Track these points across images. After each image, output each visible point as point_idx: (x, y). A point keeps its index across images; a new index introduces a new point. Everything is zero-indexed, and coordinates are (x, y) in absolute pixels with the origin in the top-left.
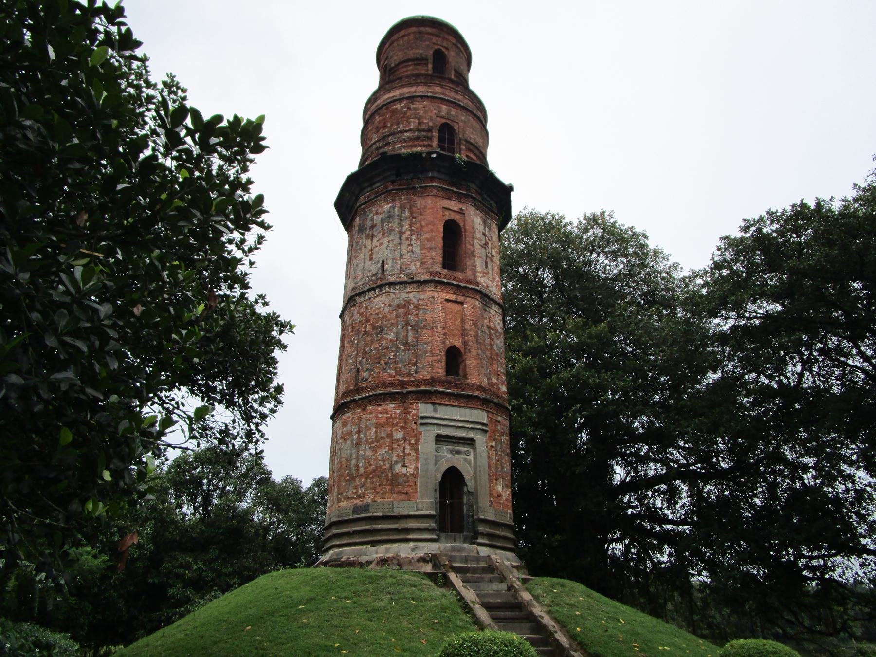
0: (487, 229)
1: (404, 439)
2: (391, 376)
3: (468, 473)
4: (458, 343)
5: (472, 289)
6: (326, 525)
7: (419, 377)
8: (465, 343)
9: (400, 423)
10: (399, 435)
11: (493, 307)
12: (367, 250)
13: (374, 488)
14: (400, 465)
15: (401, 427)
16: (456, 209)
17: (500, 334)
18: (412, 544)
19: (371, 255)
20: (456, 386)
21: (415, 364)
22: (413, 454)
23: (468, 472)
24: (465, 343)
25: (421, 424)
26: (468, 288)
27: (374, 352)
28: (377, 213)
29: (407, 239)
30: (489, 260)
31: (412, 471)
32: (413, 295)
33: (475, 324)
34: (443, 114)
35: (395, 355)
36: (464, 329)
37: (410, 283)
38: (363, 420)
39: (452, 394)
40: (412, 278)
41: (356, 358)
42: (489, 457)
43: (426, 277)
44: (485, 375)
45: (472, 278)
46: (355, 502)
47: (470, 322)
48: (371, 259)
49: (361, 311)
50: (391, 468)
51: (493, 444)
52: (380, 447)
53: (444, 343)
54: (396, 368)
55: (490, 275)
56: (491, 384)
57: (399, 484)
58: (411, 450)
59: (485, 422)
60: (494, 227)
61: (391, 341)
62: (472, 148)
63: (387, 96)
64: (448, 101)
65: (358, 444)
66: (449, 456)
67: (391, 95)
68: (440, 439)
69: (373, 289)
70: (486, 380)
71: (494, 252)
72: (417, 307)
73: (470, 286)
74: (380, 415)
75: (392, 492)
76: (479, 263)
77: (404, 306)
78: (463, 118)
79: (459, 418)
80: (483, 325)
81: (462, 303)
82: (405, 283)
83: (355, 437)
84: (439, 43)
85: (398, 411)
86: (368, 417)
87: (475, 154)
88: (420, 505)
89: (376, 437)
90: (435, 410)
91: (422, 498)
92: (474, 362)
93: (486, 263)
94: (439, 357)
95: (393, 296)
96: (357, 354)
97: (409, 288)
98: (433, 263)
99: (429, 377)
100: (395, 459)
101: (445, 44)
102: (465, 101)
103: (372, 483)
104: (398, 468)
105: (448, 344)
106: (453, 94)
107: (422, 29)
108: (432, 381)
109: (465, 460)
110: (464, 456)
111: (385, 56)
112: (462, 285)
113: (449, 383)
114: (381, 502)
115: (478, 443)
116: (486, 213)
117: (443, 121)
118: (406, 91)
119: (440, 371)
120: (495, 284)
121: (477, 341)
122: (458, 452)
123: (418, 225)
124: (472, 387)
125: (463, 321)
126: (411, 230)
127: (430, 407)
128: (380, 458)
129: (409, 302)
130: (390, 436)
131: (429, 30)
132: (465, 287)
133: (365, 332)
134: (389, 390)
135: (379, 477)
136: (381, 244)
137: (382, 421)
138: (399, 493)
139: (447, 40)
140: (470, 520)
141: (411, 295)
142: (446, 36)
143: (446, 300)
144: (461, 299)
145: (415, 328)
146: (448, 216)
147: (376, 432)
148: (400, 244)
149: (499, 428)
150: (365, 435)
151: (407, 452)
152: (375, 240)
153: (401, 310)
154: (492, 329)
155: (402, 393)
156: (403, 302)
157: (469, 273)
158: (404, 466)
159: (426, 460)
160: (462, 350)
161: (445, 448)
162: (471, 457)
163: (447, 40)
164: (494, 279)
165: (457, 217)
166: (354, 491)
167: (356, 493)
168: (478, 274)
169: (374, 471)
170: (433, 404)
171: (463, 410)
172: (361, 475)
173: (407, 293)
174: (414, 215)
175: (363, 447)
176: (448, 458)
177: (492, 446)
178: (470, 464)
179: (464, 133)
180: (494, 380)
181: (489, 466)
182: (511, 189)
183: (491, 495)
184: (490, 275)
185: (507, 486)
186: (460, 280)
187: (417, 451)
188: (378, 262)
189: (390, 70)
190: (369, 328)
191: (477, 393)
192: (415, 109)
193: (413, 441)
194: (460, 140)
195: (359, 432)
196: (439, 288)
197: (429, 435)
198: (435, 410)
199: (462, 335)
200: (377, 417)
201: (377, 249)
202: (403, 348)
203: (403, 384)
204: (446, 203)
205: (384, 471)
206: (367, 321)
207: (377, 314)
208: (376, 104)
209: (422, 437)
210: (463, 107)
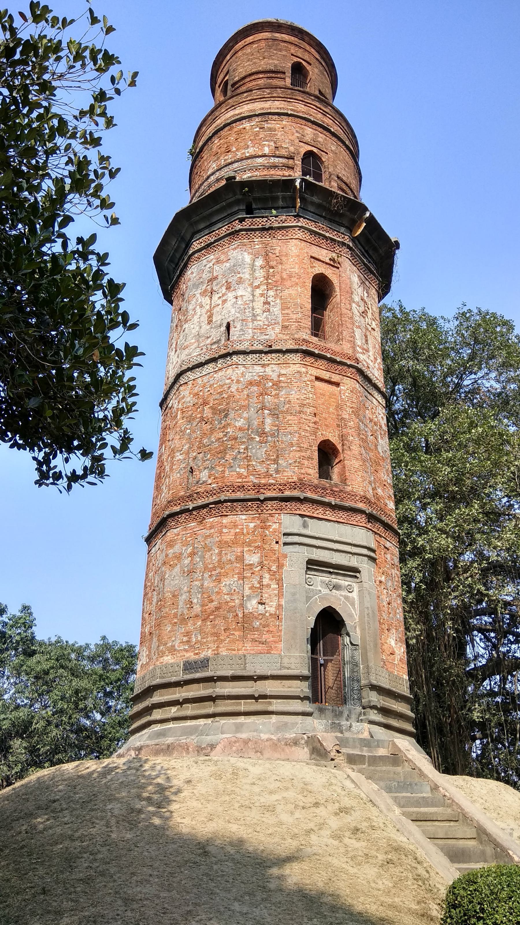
1: (261, 564)
2: (240, 476)
3: (352, 615)
6: (137, 691)
7: (282, 478)
8: (343, 438)
9: (255, 541)
10: (253, 559)
12: (204, 311)
13: (216, 635)
14: (254, 602)
15: (258, 547)
18: (274, 718)
19: (210, 317)
21: (276, 461)
22: (274, 586)
23: (351, 616)
24: (343, 438)
25: (285, 544)
27: (216, 445)
28: (218, 262)
29: (262, 295)
31: (272, 610)
32: (273, 369)
33: (356, 413)
34: (308, 138)
35: (246, 449)
37: (266, 353)
38: (200, 538)
40: (270, 346)
41: (188, 453)
43: (292, 347)
45: (350, 352)
46: (187, 655)
48: (210, 322)
49: (196, 390)
50: (242, 606)
51: (383, 579)
52: (226, 575)
53: (315, 433)
56: (376, 495)
57: (254, 629)
58: (271, 579)
59: (373, 546)
60: (373, 292)
61: (240, 429)
63: (231, 113)
64: (314, 123)
65: (191, 572)
67: (237, 112)
68: (313, 565)
69: (214, 360)
72: (277, 384)
74: (225, 530)
75: (243, 638)
77: (258, 384)
80: (365, 417)
81: (337, 384)
82: (261, 352)
83: (187, 561)
85: (252, 525)
86: (208, 532)
88: (286, 661)
89: (219, 561)
91: (289, 650)
93: (366, 337)
94: (308, 453)
95: (242, 369)
96: (190, 448)
97: (266, 359)
98: (299, 328)
99: (295, 479)
100: (247, 592)
103: (214, 626)
104: (252, 605)
106: (320, 116)
108: (301, 484)
109: (347, 598)
110: (345, 593)
111: (225, 70)
114: (228, 654)
115: (364, 575)
117: (310, 148)
118: (258, 107)
119: (312, 471)
122: (336, 587)
123: (277, 277)
125: (339, 407)
126: (268, 284)
128: (225, 590)
129: (265, 378)
130: (240, 559)
133: (202, 419)
134: (240, 495)
135: (225, 618)
136: (225, 301)
137: (228, 538)
138: (254, 640)
140: (356, 686)
141: (268, 370)
143: (318, 378)
144: (335, 378)
145: (274, 415)
146: (320, 269)
147: (220, 554)
148: (253, 301)
150: (203, 557)
151: (266, 581)
152: (215, 297)
155: (258, 499)
156: (256, 378)
159: (294, 594)
160: (339, 447)
161: (320, 579)
162: (355, 595)
164: (376, 359)
165: (329, 272)
166: (185, 639)
167: (188, 642)
169: (217, 608)
170: (302, 516)
172: (197, 616)
173: (263, 366)
174: (273, 263)
175: (198, 575)
176: (324, 592)
178: (353, 604)
182: (397, 245)
187: (279, 582)
188: (220, 326)
189: (233, 86)
190: (207, 412)
191: (361, 506)
192: (270, 129)
193: (274, 568)
194: (330, 175)
195: (192, 554)
196: (310, 360)
197: (296, 558)
198: (305, 525)
199: (338, 426)
200: (221, 532)
201: (217, 309)
202: (258, 439)
203: (258, 487)
204: (316, 251)
205: (231, 609)
206: (205, 403)
207: (221, 393)
208: (214, 125)
209: (287, 562)
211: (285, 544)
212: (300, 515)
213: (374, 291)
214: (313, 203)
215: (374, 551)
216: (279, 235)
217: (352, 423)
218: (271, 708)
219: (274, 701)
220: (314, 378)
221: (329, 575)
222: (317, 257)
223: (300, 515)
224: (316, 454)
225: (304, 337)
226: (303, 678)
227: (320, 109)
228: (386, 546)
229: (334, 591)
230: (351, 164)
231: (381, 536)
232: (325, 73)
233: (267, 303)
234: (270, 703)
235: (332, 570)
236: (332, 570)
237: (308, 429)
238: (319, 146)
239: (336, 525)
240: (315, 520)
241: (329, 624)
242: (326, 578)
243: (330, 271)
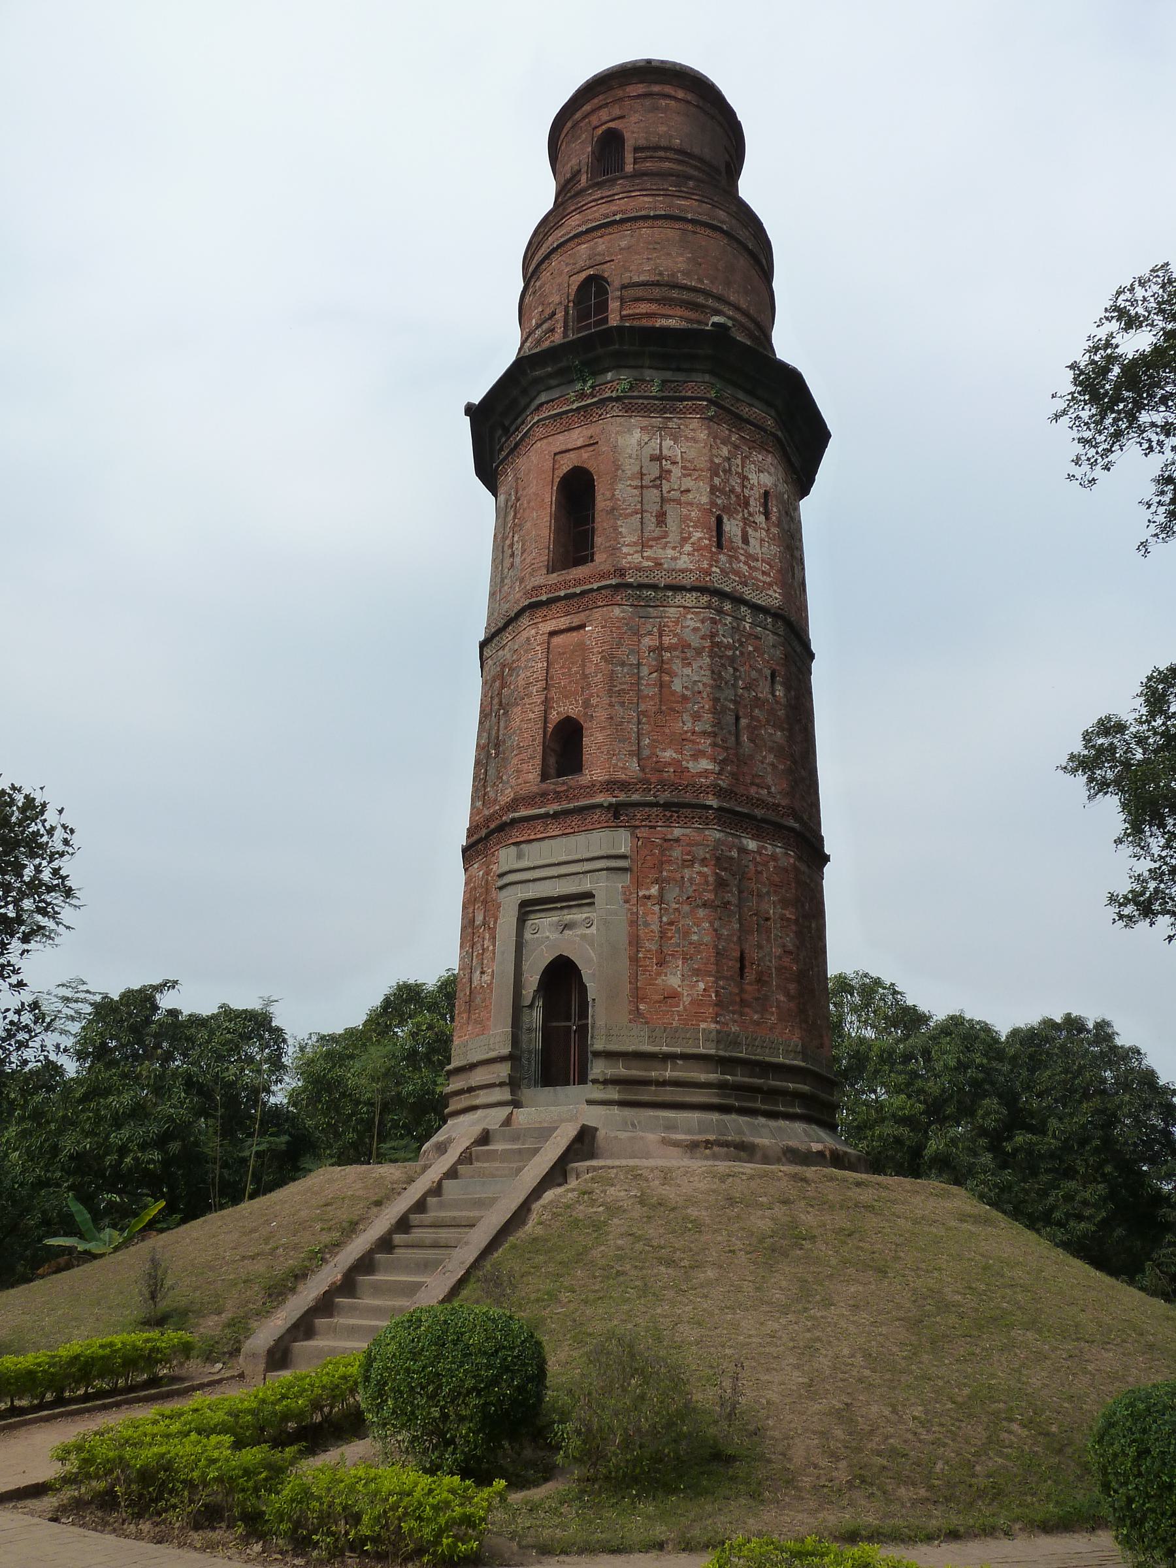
0: (668, 442)
4: (571, 708)
5: (599, 589)
11: (679, 599)
16: (579, 443)
17: (699, 652)
20: (558, 796)
22: (491, 948)
24: (586, 704)
25: (501, 888)
26: (592, 590)
30: (667, 507)
33: (608, 658)
35: (486, 771)
36: (585, 676)
39: (546, 815)
42: (634, 923)
44: (631, 753)
45: (607, 567)
47: (596, 659)
54: (485, 794)
55: (673, 537)
62: (639, 292)
66: (554, 936)
68: (527, 908)
70: (634, 765)
71: (688, 483)
73: (595, 586)
76: (628, 532)
78: (623, 244)
79: (564, 858)
84: (605, 118)
87: (650, 301)
90: (520, 856)
92: (600, 737)
101: (617, 112)
102: (633, 204)
105: (554, 717)
106: (604, 209)
107: (578, 115)
112: (578, 590)
113: (544, 794)
116: (664, 410)
117: (584, 275)
120: (688, 548)
121: (610, 692)
124: (591, 788)
127: (513, 850)
131: (587, 108)
132: (583, 593)
139: (621, 99)
142: (620, 93)
143: (552, 634)
144: (576, 621)
146: (567, 464)
149: (676, 853)
153: (497, 684)
154: (670, 649)
157: (601, 559)
158: (482, 973)
159: (503, 953)
163: (621, 99)
165: (583, 458)
168: (625, 550)
171: (572, 839)
176: (548, 938)
177: (648, 897)
179: (627, 270)
180: (668, 754)
181: (635, 942)
183: (637, 996)
184: (673, 537)
185: (697, 972)
186: (579, 582)
187: (493, 938)
191: (599, 799)
196: (540, 613)
198: (520, 856)
204: (561, 441)
210: (622, 221)
211: (501, 888)
212: (513, 844)
213: (695, 424)
214: (550, 376)
215: (624, 857)
216: (522, 449)
217: (600, 676)
218: (477, 1102)
219: (481, 1092)
220: (546, 637)
221: (558, 912)
222: (564, 448)
223: (513, 844)
224: (540, 749)
225: (536, 583)
226: (501, 1059)
227: (602, 198)
228: (669, 837)
229: (566, 932)
230: (670, 233)
231: (651, 827)
232: (663, 102)
233: (512, 555)
234: (477, 1096)
235: (559, 905)
236: (559, 905)
237: (532, 716)
238: (599, 259)
239: (564, 840)
240: (535, 844)
241: (562, 977)
242: (554, 918)
243: (585, 456)
